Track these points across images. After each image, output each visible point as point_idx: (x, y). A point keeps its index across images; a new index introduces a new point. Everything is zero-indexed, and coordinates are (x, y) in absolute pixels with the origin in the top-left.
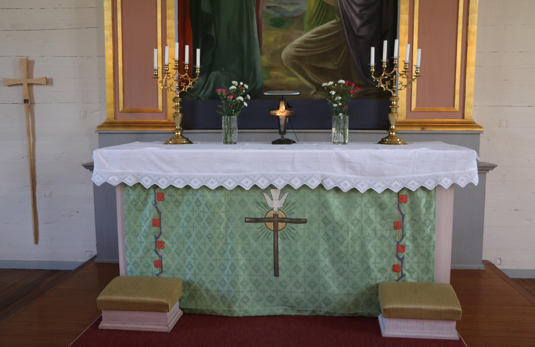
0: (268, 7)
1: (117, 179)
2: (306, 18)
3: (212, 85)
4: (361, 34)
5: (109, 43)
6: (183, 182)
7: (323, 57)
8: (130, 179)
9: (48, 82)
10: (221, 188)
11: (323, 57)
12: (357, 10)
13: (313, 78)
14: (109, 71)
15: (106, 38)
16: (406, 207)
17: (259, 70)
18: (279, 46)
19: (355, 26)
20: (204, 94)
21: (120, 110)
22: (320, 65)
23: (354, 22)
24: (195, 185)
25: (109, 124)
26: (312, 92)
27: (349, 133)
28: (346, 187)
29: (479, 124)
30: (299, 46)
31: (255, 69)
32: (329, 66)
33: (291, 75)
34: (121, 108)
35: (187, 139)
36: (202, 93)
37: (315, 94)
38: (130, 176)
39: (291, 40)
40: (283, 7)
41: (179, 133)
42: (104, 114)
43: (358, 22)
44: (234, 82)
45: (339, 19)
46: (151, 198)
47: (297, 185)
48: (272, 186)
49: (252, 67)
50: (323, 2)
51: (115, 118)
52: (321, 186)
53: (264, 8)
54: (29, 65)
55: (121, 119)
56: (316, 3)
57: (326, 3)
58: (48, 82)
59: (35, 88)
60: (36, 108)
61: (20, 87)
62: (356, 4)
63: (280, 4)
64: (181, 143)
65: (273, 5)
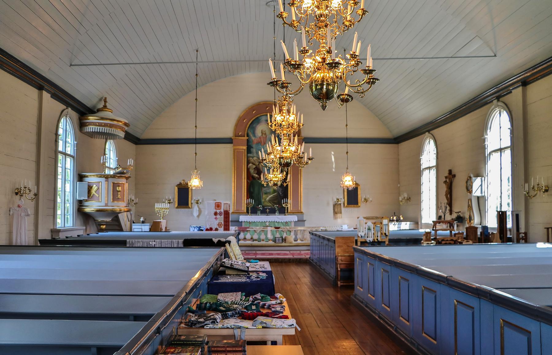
49: (261, 202)
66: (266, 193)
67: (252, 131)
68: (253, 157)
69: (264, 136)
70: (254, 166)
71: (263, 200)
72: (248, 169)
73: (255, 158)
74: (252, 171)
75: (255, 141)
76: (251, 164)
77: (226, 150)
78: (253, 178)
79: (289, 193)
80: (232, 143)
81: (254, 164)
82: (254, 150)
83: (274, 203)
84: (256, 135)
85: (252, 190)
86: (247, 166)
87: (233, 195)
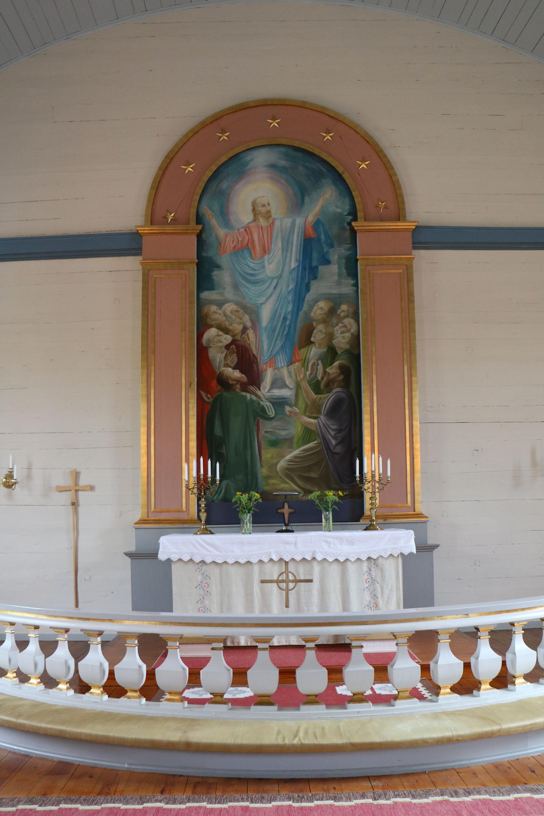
0: (266, 432)
2: (295, 440)
3: (223, 491)
4: (336, 451)
7: (309, 469)
9: (92, 488)
11: (309, 469)
12: (333, 433)
17: (260, 480)
18: (275, 461)
19: (332, 444)
20: (217, 497)
21: (152, 510)
22: (307, 475)
25: (143, 521)
29: (426, 515)
30: (290, 461)
31: (257, 478)
32: (313, 475)
34: (152, 509)
36: (215, 497)
37: (303, 496)
39: (284, 457)
40: (277, 431)
42: (138, 514)
43: (334, 442)
45: (319, 440)
49: (255, 477)
51: (148, 517)
53: (263, 432)
54: (76, 475)
55: (152, 518)
58: (92, 488)
59: (80, 493)
60: (81, 509)
61: (69, 493)
62: (331, 429)
63: (275, 429)
66: (274, 444)
68: (220, 304)
69: (262, 222)
70: (228, 339)
71: (263, 471)
72: (202, 352)
73: (229, 307)
74: (217, 356)
75: (229, 244)
76: (213, 332)
77: (115, 281)
79: (367, 439)
81: (226, 331)
82: (224, 276)
84: (232, 218)
85: (218, 431)
86: (200, 336)
87: (144, 450)
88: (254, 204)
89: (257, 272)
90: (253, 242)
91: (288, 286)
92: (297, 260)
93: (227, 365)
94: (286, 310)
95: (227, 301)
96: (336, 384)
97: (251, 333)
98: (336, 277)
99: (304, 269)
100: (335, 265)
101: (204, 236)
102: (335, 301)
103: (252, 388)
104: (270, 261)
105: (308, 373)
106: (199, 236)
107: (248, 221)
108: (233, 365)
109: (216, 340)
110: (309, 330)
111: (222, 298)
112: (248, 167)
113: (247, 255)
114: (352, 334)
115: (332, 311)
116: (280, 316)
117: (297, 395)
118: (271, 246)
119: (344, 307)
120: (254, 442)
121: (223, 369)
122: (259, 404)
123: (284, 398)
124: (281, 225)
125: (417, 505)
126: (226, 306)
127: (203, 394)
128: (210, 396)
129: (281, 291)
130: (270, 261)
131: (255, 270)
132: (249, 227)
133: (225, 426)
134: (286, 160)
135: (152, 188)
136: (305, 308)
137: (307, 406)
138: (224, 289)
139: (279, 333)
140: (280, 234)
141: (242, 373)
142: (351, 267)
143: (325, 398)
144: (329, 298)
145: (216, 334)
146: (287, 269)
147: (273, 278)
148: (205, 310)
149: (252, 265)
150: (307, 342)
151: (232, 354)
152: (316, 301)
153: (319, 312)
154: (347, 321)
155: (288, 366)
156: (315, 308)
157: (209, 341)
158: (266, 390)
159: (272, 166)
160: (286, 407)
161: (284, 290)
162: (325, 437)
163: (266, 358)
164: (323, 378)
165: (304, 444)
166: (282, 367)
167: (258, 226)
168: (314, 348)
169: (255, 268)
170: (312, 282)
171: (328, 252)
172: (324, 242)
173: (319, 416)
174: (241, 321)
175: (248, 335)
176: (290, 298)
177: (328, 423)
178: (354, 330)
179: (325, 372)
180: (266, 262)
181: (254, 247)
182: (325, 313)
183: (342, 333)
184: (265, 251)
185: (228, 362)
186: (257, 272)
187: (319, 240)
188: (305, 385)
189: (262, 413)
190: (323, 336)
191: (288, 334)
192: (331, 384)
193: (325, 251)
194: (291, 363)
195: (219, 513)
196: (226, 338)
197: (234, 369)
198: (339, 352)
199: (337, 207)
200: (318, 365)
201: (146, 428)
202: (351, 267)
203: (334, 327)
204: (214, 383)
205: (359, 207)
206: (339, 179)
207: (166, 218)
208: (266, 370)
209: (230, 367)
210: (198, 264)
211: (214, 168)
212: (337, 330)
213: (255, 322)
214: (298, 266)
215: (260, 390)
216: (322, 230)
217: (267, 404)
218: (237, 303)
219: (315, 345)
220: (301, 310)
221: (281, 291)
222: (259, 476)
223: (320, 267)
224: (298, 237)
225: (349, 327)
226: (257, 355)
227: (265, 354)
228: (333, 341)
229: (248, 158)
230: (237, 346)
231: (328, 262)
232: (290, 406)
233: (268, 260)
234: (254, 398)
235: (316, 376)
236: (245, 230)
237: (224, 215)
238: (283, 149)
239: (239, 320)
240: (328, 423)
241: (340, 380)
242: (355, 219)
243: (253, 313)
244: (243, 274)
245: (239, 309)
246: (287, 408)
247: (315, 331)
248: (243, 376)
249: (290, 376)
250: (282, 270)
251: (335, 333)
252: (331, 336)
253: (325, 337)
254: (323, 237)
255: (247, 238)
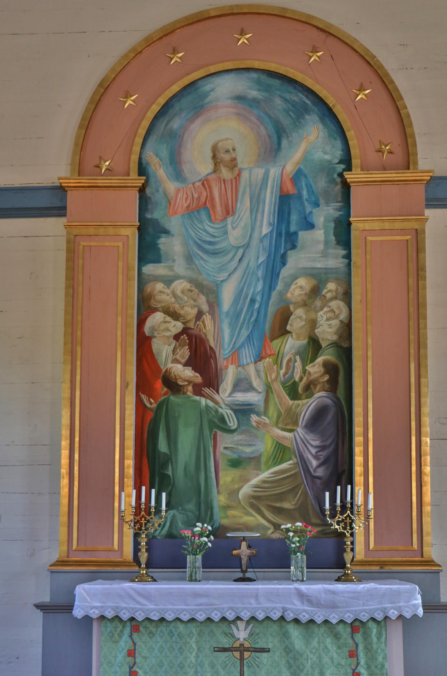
0: (225, 448)
1: (97, 612)
2: (263, 459)
3: (168, 524)
4: (317, 474)
5: (65, 482)
6: (158, 614)
7: (281, 497)
8: (110, 612)
10: (193, 620)
11: (281, 497)
12: (313, 451)
13: (271, 518)
14: (64, 508)
15: (62, 476)
16: (359, 637)
17: (216, 510)
18: (236, 486)
19: (312, 467)
20: (160, 533)
21: (74, 548)
22: (278, 505)
23: (311, 463)
24: (169, 617)
26: (270, 532)
27: (307, 572)
28: (304, 618)
29: (439, 563)
30: (256, 486)
31: (212, 508)
32: (287, 505)
33: (249, 514)
34: (75, 546)
35: (152, 578)
37: (273, 533)
38: (109, 610)
39: (248, 480)
40: (240, 448)
41: (145, 572)
43: (315, 463)
44: (198, 524)
45: (295, 460)
46: (127, 630)
47: (261, 616)
48: (239, 618)
49: (210, 507)
50: (280, 444)
51: (68, 557)
52: (282, 618)
53: (222, 448)
56: (273, 444)
57: (283, 445)
62: (312, 445)
63: (238, 445)
64: (146, 581)
65: (230, 446)
66: (235, 463)
67: (165, 152)
68: (168, 281)
69: (225, 173)
71: (219, 500)
72: (144, 343)
73: (180, 286)
78: (172, 385)
79: (358, 459)
80: (60, 211)
81: (175, 316)
82: (172, 245)
83: (279, 511)
84: (186, 169)
86: (141, 323)
88: (215, 150)
89: (217, 239)
90: (212, 199)
91: (258, 258)
92: (270, 224)
93: (176, 361)
94: (254, 290)
95: (177, 277)
96: (318, 388)
97: (207, 318)
98: (321, 247)
99: (279, 235)
100: (321, 230)
101: (148, 191)
102: (319, 279)
103: (207, 390)
104: (234, 225)
105: (282, 372)
106: (142, 190)
107: (206, 172)
108: (183, 361)
109: (162, 328)
110: (284, 317)
111: (171, 273)
112: (207, 100)
113: (204, 216)
114: (341, 321)
115: (315, 291)
116: (246, 297)
117: (267, 401)
118: (236, 206)
119: (331, 286)
120: (209, 462)
121: (170, 365)
122: (217, 411)
123: (250, 405)
124: (250, 177)
125: (425, 549)
126: (176, 283)
127: (144, 398)
128: (152, 401)
129: (248, 264)
130: (234, 225)
131: (214, 237)
132: (207, 180)
133: (172, 440)
134: (259, 90)
135: (80, 127)
136: (280, 287)
137: (279, 415)
138: (174, 261)
139: (244, 320)
140: (248, 190)
141: (195, 372)
142: (343, 232)
143: (303, 405)
144: (310, 273)
145: (162, 320)
146: (256, 235)
147: (238, 248)
148: (148, 288)
149: (211, 230)
150: (281, 329)
151: (182, 347)
152: (295, 278)
153: (298, 292)
154: (334, 304)
155: (256, 362)
156: (293, 287)
157: (153, 329)
158: (226, 395)
159: (240, 98)
160: (252, 415)
161: (253, 264)
162: (303, 456)
163: (227, 352)
164: (301, 379)
165: (275, 464)
166: (248, 364)
167: (219, 178)
168: (290, 339)
169: (215, 234)
170: (289, 252)
171: (311, 212)
172: (306, 200)
173: (295, 428)
174: (195, 303)
175: (203, 322)
176: (260, 273)
177: (308, 437)
178: (343, 316)
179: (304, 371)
180: (229, 227)
181: (213, 206)
182: (305, 294)
183: (328, 320)
184: (229, 211)
185: (178, 357)
186: (217, 239)
187: (300, 196)
188: (278, 387)
189: (220, 424)
190: (303, 323)
191: (256, 320)
192: (312, 386)
193: (308, 211)
194: (259, 358)
195: (163, 556)
196: (175, 326)
197: (184, 366)
198: (324, 345)
199: (325, 153)
200: (296, 361)
201: (68, 441)
202: (343, 232)
203: (317, 312)
204: (159, 384)
205: (354, 152)
206: (328, 114)
207: (98, 166)
208: (227, 367)
209: (179, 362)
210: (139, 229)
211: (162, 101)
212: (322, 316)
213: (214, 305)
214: (271, 232)
215: (218, 392)
216: (304, 184)
217: (227, 412)
218: (191, 281)
219: (292, 336)
220: (274, 290)
221: (248, 264)
222: (216, 505)
223: (301, 234)
224: (272, 193)
225: (337, 312)
226: (216, 347)
227: (226, 347)
228: (316, 331)
229: (207, 88)
230: (190, 337)
231: (311, 226)
232: (258, 414)
233: (232, 223)
234: (211, 404)
235: (292, 376)
236: (203, 184)
237: (175, 163)
238: (254, 75)
239: (192, 302)
240: (308, 437)
241: (324, 382)
242: (349, 168)
243: (212, 293)
244: (199, 242)
245: (193, 288)
246: (254, 418)
247: (292, 317)
248: (197, 374)
249: (259, 376)
250: (251, 236)
251: (319, 319)
252: (313, 324)
253: (305, 325)
254: (305, 193)
255: (204, 194)
